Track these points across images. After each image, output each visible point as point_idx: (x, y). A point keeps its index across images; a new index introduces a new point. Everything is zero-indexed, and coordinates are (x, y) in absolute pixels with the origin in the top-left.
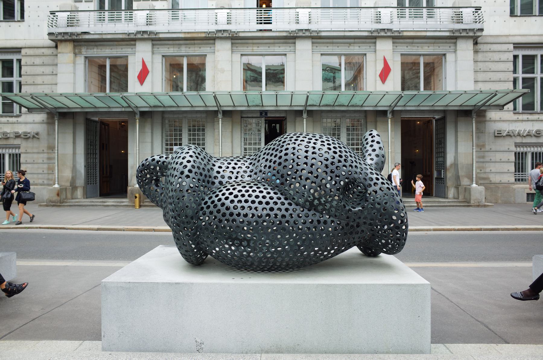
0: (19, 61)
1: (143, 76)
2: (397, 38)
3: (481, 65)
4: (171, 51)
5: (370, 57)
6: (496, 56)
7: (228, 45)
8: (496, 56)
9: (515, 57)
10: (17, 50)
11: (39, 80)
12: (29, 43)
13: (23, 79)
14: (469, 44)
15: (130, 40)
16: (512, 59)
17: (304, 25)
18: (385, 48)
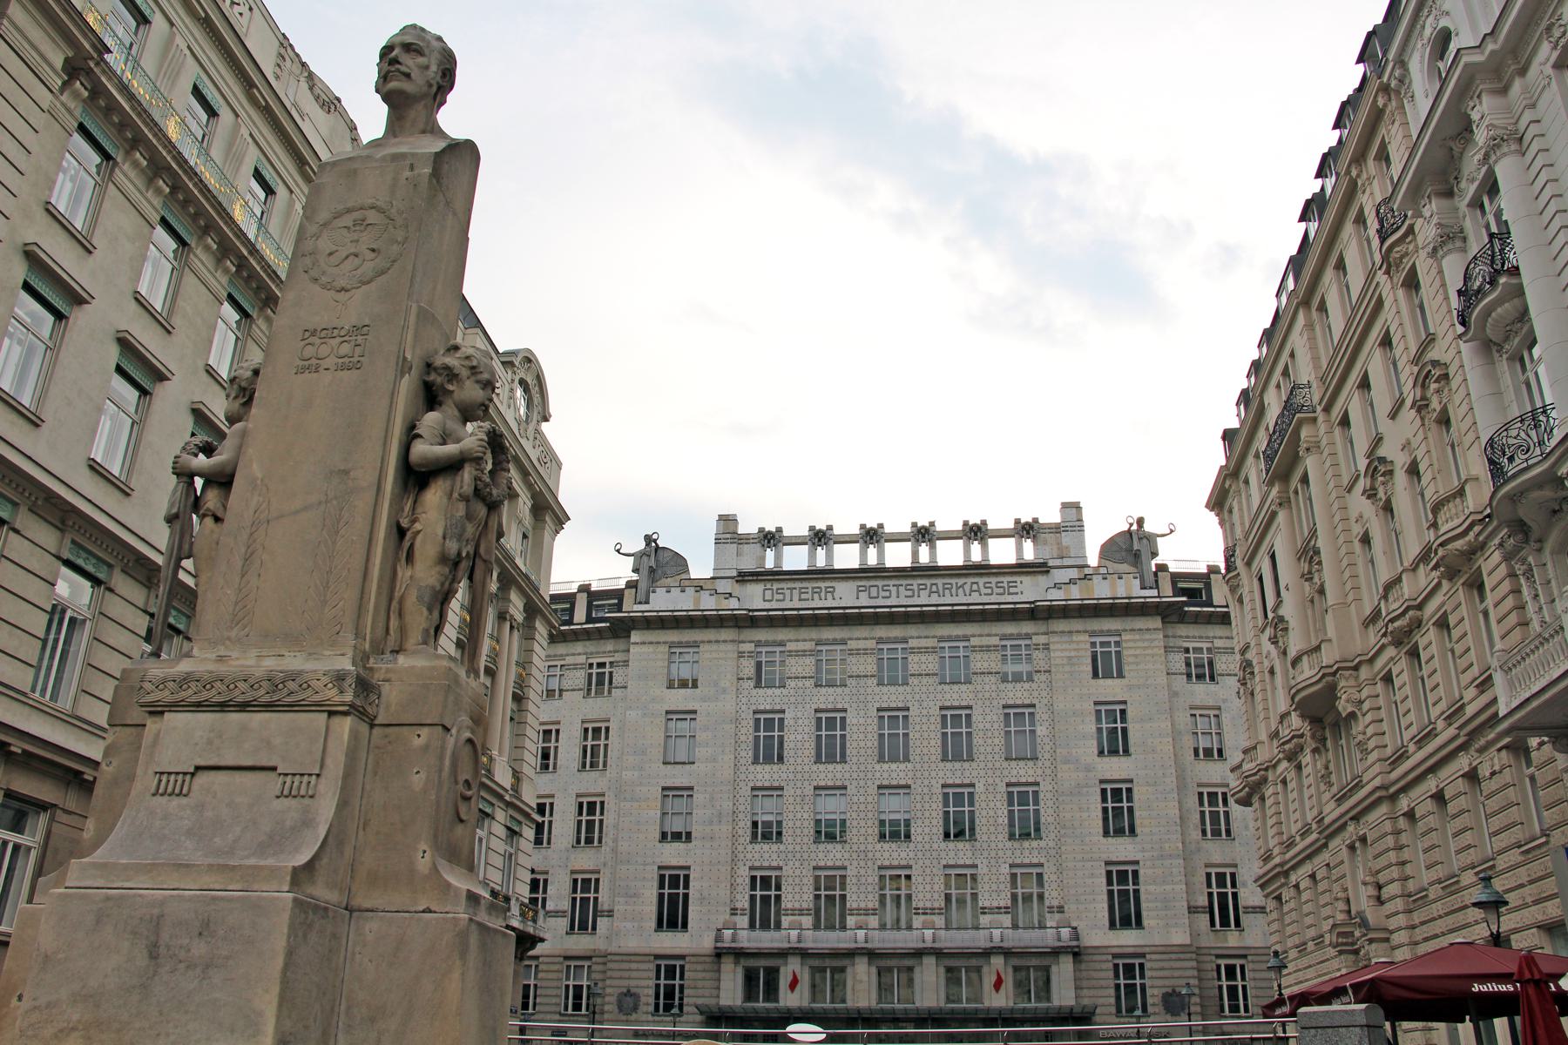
0: (682, 967)
1: (793, 984)
2: (1007, 953)
3: (1084, 974)
4: (817, 963)
5: (985, 970)
6: (1097, 966)
7: (865, 959)
8: (1097, 966)
9: (1116, 966)
10: (682, 957)
11: (700, 984)
12: (692, 951)
13: (686, 983)
14: (1070, 958)
15: (783, 954)
16: (1110, 965)
17: (929, 944)
18: (998, 962)
